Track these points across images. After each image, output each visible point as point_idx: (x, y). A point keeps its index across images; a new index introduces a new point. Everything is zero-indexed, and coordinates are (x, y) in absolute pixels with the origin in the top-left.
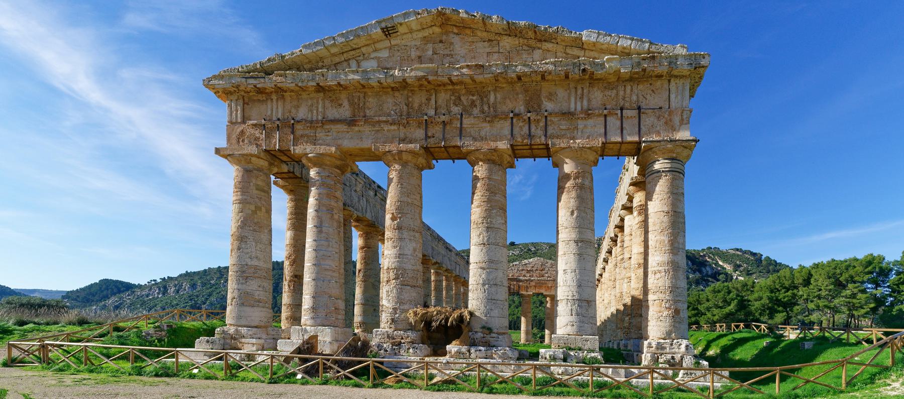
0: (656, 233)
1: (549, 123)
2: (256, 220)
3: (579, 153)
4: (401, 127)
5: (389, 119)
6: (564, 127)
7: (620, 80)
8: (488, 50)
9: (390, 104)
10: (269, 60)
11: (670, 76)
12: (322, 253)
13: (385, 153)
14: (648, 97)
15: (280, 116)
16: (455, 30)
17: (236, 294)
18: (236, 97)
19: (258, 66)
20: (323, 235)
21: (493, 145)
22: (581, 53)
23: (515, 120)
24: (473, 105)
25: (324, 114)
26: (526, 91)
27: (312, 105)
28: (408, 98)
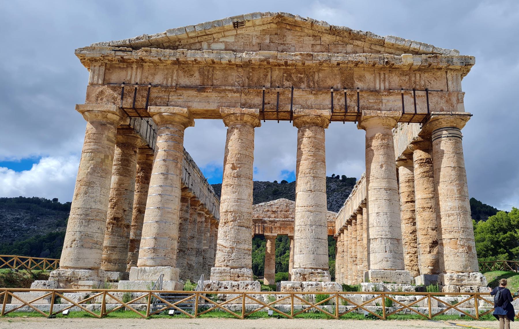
0: (446, 184)
1: (360, 97)
2: (104, 167)
3: (385, 120)
4: (243, 95)
5: (234, 88)
6: (372, 101)
7: (412, 70)
8: (313, 42)
9: (234, 76)
10: (137, 39)
11: (447, 70)
12: (166, 197)
13: (229, 115)
14: (432, 82)
15: (138, 81)
16: (288, 27)
17: (77, 236)
18: (100, 64)
19: (128, 42)
20: (169, 181)
21: (319, 112)
22: (382, 49)
23: (334, 94)
24: (301, 80)
25: (177, 82)
26: (342, 73)
27: (167, 74)
28: (249, 72)
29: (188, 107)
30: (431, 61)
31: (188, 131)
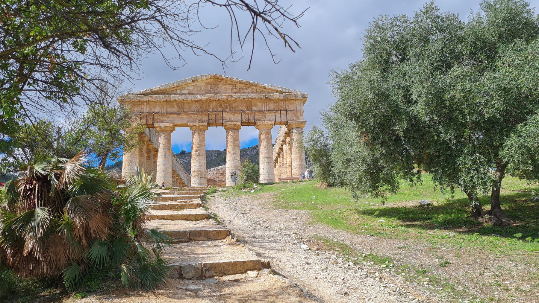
7: (279, 101)
9: (194, 107)
11: (296, 100)
13: (193, 126)
15: (147, 111)
21: (235, 123)
24: (226, 107)
26: (246, 103)
29: (173, 123)
30: (287, 96)
31: (173, 133)
